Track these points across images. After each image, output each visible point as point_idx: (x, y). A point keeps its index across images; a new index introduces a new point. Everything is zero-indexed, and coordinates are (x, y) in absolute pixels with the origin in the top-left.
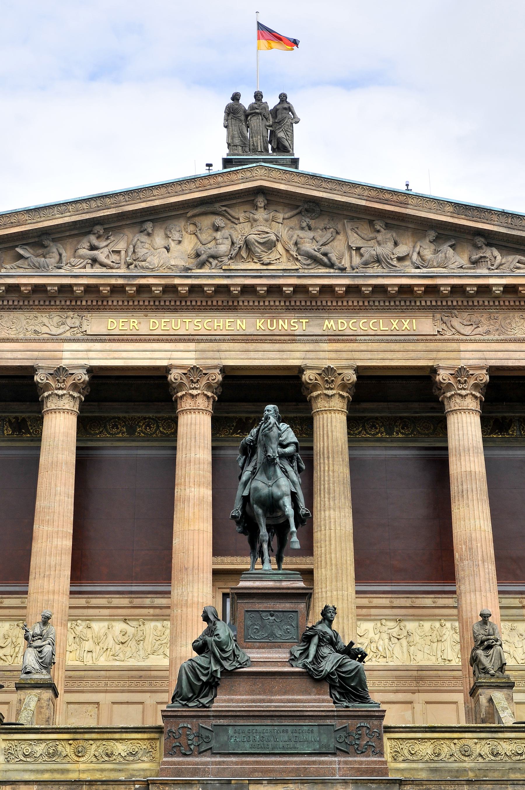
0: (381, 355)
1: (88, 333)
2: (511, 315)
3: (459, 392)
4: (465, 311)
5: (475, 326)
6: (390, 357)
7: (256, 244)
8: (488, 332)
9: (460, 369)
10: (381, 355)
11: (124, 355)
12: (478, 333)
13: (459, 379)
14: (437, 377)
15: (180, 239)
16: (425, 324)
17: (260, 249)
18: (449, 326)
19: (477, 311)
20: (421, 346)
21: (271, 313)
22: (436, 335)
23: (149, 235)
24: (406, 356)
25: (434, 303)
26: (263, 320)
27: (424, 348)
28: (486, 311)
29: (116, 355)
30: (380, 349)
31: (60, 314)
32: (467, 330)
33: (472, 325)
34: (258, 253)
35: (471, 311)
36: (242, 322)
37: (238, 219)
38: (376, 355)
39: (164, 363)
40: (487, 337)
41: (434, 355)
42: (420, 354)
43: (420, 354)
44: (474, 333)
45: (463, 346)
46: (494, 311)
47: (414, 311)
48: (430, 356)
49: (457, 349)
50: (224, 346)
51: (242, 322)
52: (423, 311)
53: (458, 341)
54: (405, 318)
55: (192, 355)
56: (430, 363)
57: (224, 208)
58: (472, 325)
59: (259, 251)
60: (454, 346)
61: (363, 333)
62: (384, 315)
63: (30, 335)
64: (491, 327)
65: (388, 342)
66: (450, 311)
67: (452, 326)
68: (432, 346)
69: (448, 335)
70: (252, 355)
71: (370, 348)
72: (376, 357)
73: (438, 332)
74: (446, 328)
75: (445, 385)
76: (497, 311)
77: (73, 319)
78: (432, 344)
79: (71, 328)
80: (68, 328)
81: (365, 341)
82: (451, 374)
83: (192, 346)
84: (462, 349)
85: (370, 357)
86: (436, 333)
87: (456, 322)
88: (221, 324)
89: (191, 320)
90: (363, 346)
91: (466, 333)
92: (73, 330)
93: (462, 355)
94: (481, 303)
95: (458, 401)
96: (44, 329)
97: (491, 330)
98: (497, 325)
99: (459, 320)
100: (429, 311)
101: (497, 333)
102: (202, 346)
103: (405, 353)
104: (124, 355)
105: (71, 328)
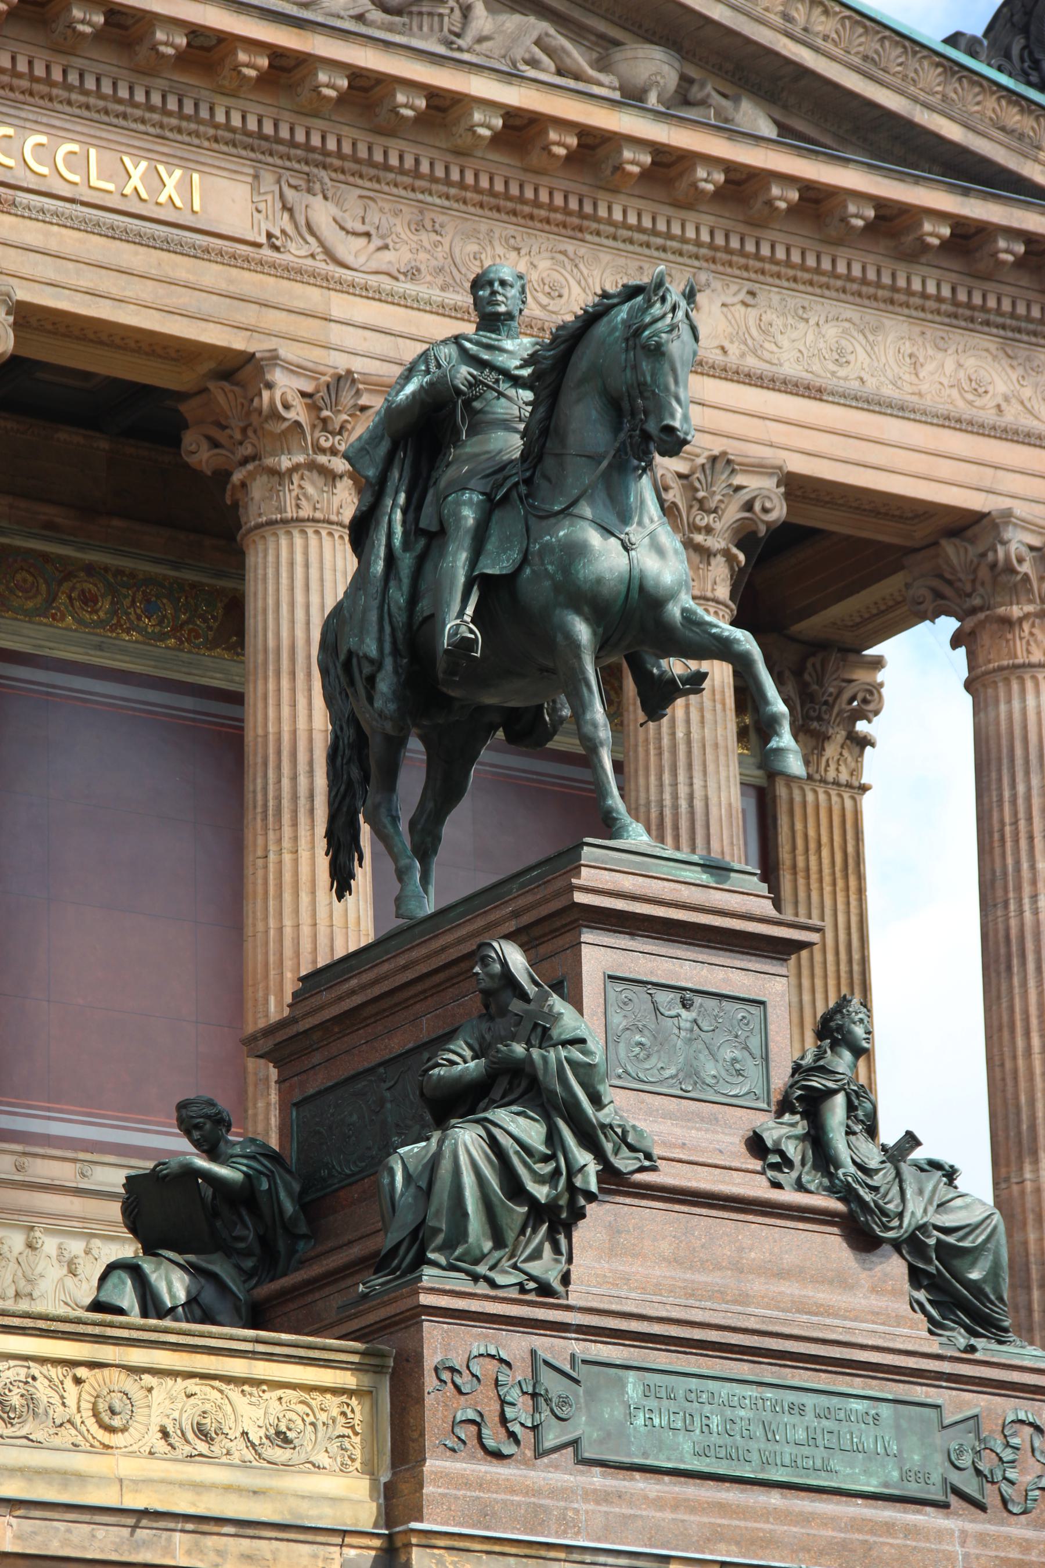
0: (88, 279)
2: (484, 226)
3: (322, 459)
4: (351, 179)
5: (377, 242)
6: (115, 291)
8: (412, 274)
9: (339, 378)
10: (88, 279)
12: (384, 267)
13: (326, 413)
14: (266, 395)
16: (221, 196)
18: (302, 222)
19: (386, 188)
20: (212, 274)
22: (259, 245)
24: (168, 301)
25: (268, 129)
27: (223, 286)
28: (412, 195)
30: (84, 256)
32: (349, 248)
33: (368, 235)
35: (368, 184)
38: (70, 274)
40: (404, 286)
41: (249, 315)
42: (210, 304)
43: (210, 304)
44: (373, 265)
45: (340, 305)
46: (438, 201)
47: (196, 141)
48: (243, 320)
49: (320, 309)
52: (225, 148)
53: (326, 283)
54: (172, 161)
56: (238, 342)
58: (368, 235)
60: (311, 296)
61: (32, 183)
62: (104, 135)
64: (422, 256)
65: (113, 234)
66: (306, 169)
67: (308, 225)
68: (248, 282)
69: (296, 252)
71: (53, 246)
72: (73, 281)
73: (269, 235)
74: (290, 229)
75: (286, 424)
76: (446, 203)
78: (247, 274)
81: (40, 216)
82: (304, 394)
84: (336, 313)
85: (51, 275)
86: (263, 239)
87: (322, 212)
90: (31, 233)
91: (350, 260)
93: (337, 334)
94: (409, 163)
95: (310, 490)
97: (423, 268)
98: (440, 253)
99: (332, 209)
100: (243, 153)
101: (440, 281)
103: (162, 290)
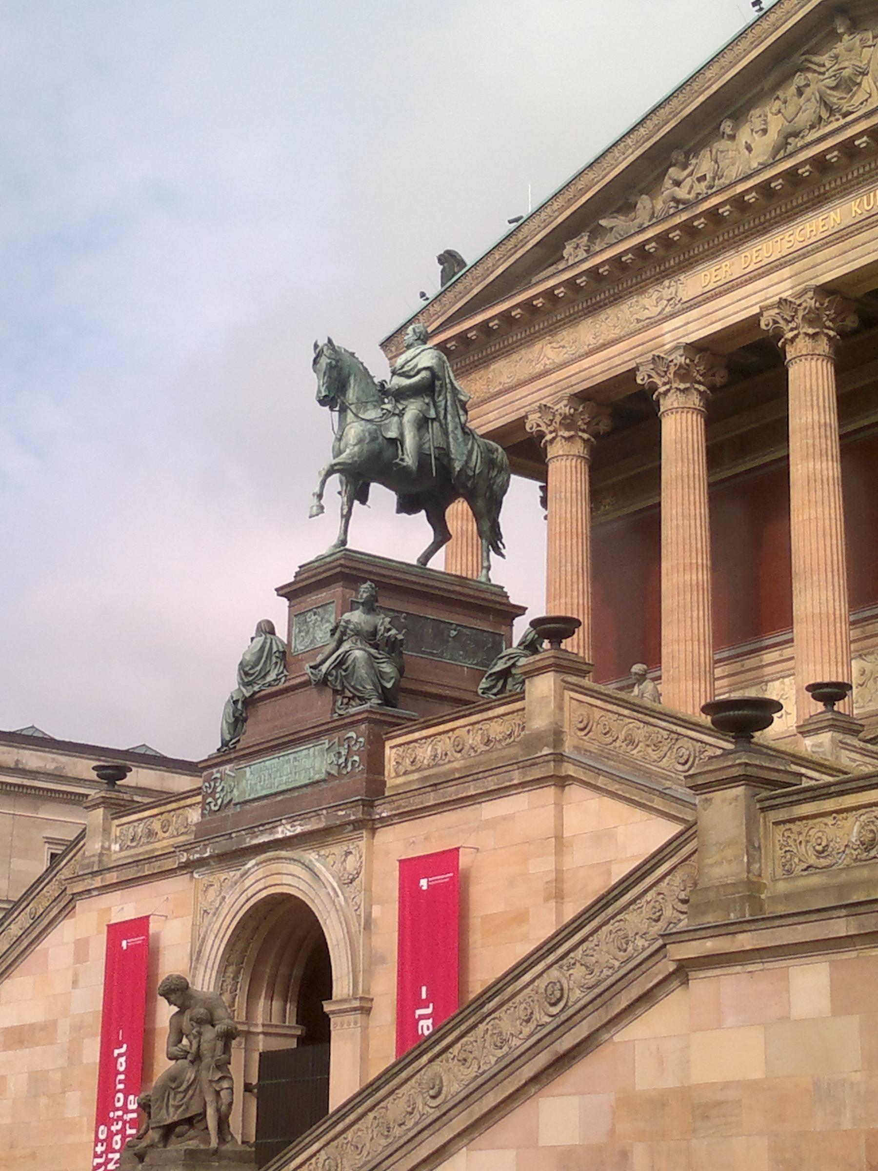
1: (684, 300)
7: (829, 91)
11: (721, 314)
15: (763, 127)
17: (835, 96)
21: (868, 184)
23: (732, 137)
26: (858, 200)
29: (713, 317)
31: (657, 288)
34: (835, 104)
36: (836, 214)
37: (824, 66)
39: (756, 310)
50: (820, 256)
51: (836, 214)
55: (788, 284)
57: (803, 57)
59: (835, 100)
63: (635, 326)
70: (851, 255)
77: (667, 289)
79: (669, 300)
80: (665, 302)
83: (786, 272)
88: (814, 228)
89: (782, 237)
92: (671, 302)
96: (647, 314)
102: (798, 266)
104: (721, 314)
105: (669, 300)
